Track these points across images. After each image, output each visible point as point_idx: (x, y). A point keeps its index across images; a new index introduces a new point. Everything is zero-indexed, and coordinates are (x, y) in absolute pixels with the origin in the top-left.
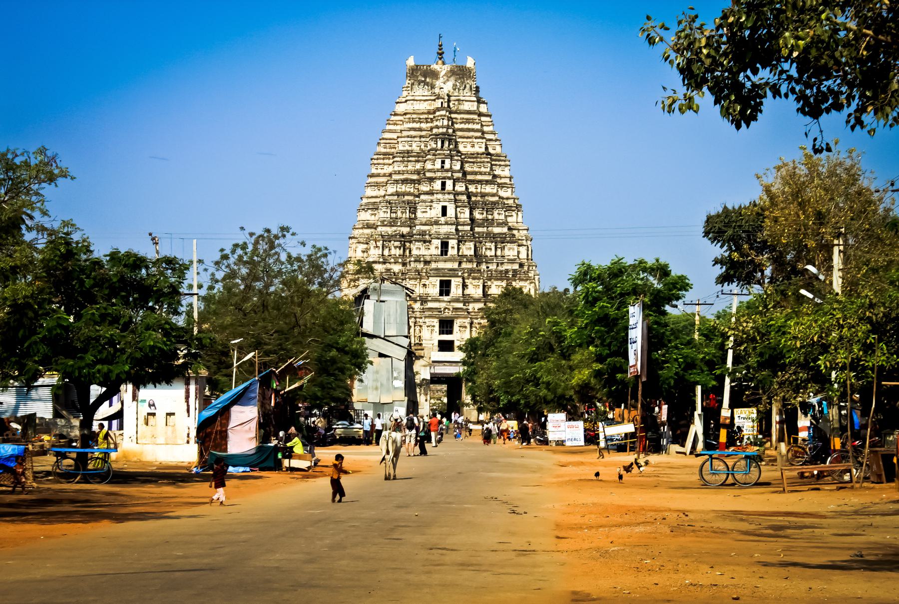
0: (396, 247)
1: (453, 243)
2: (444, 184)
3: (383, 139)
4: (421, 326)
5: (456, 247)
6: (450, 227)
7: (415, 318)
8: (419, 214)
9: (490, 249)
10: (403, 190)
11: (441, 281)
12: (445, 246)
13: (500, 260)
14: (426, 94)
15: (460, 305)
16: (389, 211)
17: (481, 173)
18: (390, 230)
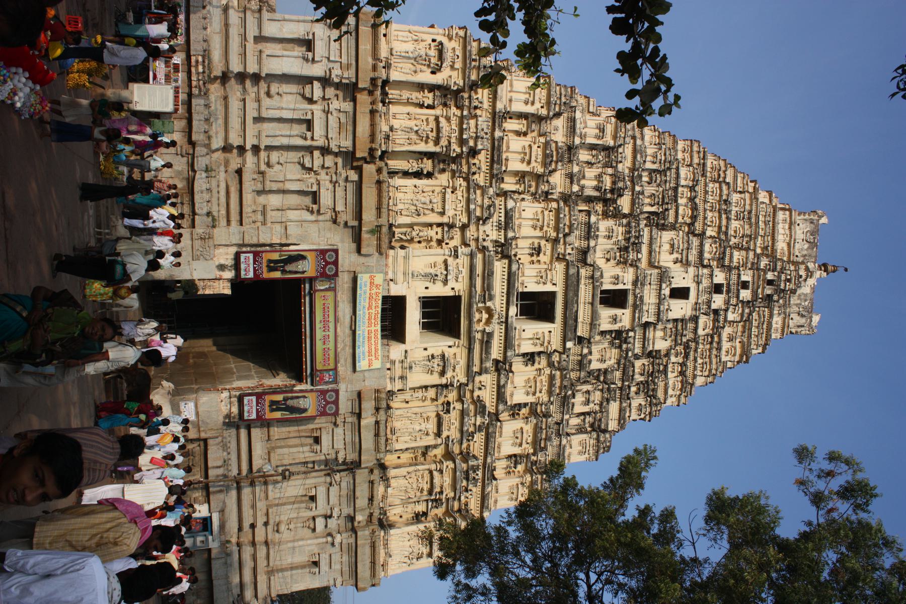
0: (599, 177)
1: (625, 317)
2: (718, 289)
3: (726, 166)
4: (440, 242)
5: (616, 327)
6: (653, 309)
7: (464, 227)
8: (667, 236)
9: (587, 402)
10: (680, 201)
11: (553, 294)
12: (615, 299)
14: (797, 246)
16: (654, 167)
17: (695, 360)
18: (624, 167)
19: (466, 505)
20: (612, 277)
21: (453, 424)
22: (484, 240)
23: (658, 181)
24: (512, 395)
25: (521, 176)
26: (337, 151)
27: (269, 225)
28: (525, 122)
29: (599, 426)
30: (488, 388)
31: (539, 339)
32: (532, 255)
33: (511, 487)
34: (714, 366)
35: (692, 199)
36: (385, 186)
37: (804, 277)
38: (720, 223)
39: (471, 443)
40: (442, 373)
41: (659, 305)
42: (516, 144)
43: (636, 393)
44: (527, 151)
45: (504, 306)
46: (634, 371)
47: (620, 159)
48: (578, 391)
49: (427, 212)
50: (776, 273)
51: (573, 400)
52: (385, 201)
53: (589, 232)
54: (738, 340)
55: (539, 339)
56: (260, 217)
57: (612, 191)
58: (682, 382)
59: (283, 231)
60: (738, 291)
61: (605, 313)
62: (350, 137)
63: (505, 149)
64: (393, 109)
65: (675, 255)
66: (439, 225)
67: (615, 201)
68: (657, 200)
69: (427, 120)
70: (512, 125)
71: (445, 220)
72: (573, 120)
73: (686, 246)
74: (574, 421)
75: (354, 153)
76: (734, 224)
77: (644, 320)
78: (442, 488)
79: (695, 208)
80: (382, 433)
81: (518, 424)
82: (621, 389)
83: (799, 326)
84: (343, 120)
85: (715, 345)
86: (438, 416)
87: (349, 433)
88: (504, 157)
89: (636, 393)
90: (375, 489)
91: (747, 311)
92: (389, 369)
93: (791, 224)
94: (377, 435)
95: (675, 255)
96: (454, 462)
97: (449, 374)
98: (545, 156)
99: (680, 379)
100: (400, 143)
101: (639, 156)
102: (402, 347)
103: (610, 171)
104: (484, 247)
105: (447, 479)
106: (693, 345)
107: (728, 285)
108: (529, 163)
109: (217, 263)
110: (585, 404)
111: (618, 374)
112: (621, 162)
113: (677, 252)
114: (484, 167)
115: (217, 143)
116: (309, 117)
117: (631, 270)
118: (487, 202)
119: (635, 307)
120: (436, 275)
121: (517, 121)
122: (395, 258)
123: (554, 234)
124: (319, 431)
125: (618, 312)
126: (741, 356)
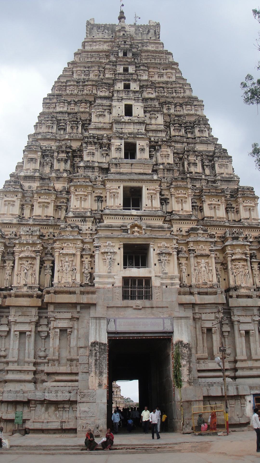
0: (58, 160)
1: (141, 144)
2: (127, 87)
5: (147, 149)
6: (138, 127)
7: (83, 242)
8: (94, 119)
9: (195, 164)
10: (76, 110)
11: (124, 188)
12: (130, 151)
13: (211, 178)
14: (106, 37)
15: (160, 223)
16: (55, 127)
17: (173, 98)
18: (54, 145)
19: (256, 238)
20: (116, 153)
21: (202, 247)
22: (92, 230)
23: (64, 125)
24: (186, 211)
25: (57, 208)
26: (38, 317)
27: (78, 357)
28: (25, 207)
29: (211, 156)
30: (181, 226)
31: (152, 197)
32: (102, 201)
33: (246, 210)
34: (178, 85)
35: (76, 103)
36: (57, 289)
37: (124, 33)
38: (90, 85)
39: (216, 235)
40: (170, 254)
41: (134, 123)
42: (38, 211)
43: (192, 134)
44: (42, 205)
45: (131, 217)
46: (178, 136)
47: (49, 148)
48: (188, 170)
49: (74, 264)
50: (119, 51)
51: (194, 173)
52: (65, 289)
53: (89, 167)
54: (162, 71)
55: (152, 197)
56: (74, 362)
57: (67, 153)
58: (186, 105)
59: (82, 350)
60: (128, 74)
61: (139, 155)
62: (30, 309)
63: (40, 218)
64: (15, 284)
65: (106, 113)
66: (82, 256)
67: (74, 151)
68: (74, 125)
69: (21, 264)
70: (27, 213)
71: (79, 253)
72: (26, 178)
73: (101, 107)
74: (207, 172)
75: (40, 308)
76: (92, 76)
77: (143, 131)
78: (243, 253)
79: (81, 102)
80: (205, 290)
81: (206, 207)
82: (188, 143)
83: (155, 34)
84: (20, 314)
85: (164, 85)
86: (196, 257)
87: (205, 311)
88: (45, 218)
89: (192, 134)
90: (242, 294)
91: (142, 68)
92: (167, 287)
93: (93, 42)
94: (206, 294)
95: (106, 113)
96: (227, 246)
97: (170, 251)
98: (45, 194)
99: (184, 107)
100: (32, 280)
101: (48, 137)
102: (153, 279)
103: (56, 154)
104: (96, 230)
105: (237, 250)
106: (162, 100)
107: (124, 80)
108: (49, 203)
109: (98, 388)
110: (197, 165)
111: (179, 146)
112: (51, 147)
113: (104, 112)
114: (51, 230)
115: (31, 386)
116: (18, 333)
117: (113, 141)
118: (69, 229)
119: (134, 138)
120: (111, 258)
121: (25, 211)
122: (99, 283)
123: (90, 188)
124: (203, 329)
125: (138, 147)
126: (173, 69)
